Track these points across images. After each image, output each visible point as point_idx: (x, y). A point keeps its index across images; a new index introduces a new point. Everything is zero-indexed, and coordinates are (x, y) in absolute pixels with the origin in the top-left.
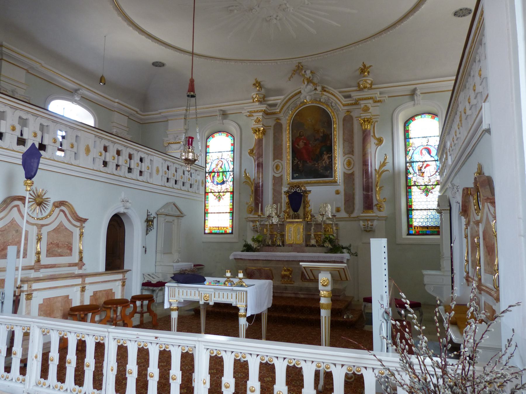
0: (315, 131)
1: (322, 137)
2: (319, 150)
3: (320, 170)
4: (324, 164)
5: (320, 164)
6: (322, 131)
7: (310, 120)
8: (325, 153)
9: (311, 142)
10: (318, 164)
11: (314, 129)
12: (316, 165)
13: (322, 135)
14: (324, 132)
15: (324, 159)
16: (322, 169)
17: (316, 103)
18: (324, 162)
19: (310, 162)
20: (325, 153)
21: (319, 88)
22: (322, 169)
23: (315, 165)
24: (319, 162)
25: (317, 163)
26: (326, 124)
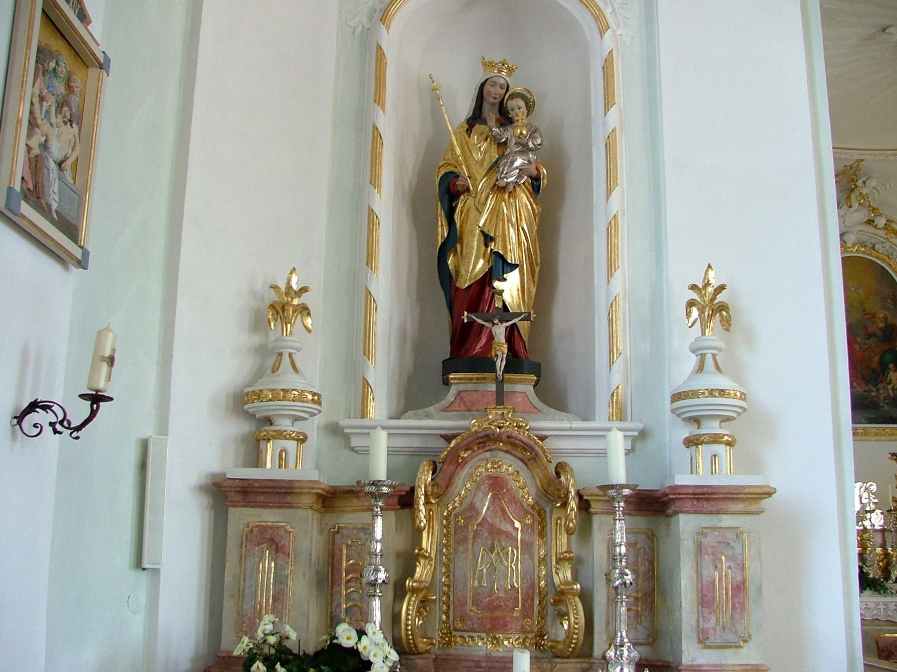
0: (865, 314)
1: (882, 329)
2: (876, 358)
3: (881, 404)
4: (891, 392)
5: (881, 392)
6: (882, 315)
7: (852, 289)
8: (891, 366)
9: (859, 340)
10: (878, 390)
11: (864, 310)
12: (873, 394)
13: (881, 325)
14: (886, 318)
15: (891, 380)
16: (887, 404)
17: (864, 253)
18: (890, 387)
19: (858, 384)
20: (891, 366)
21: (881, 222)
22: (887, 404)
23: (870, 393)
24: (880, 386)
25: (874, 389)
26: (888, 301)
